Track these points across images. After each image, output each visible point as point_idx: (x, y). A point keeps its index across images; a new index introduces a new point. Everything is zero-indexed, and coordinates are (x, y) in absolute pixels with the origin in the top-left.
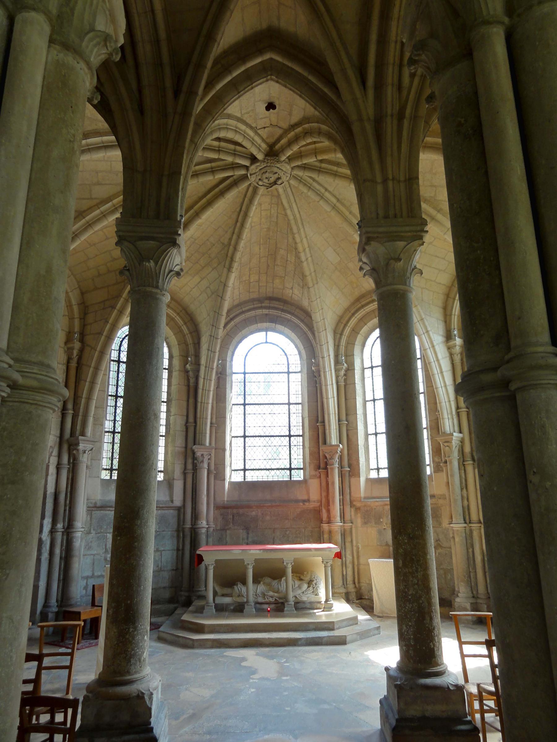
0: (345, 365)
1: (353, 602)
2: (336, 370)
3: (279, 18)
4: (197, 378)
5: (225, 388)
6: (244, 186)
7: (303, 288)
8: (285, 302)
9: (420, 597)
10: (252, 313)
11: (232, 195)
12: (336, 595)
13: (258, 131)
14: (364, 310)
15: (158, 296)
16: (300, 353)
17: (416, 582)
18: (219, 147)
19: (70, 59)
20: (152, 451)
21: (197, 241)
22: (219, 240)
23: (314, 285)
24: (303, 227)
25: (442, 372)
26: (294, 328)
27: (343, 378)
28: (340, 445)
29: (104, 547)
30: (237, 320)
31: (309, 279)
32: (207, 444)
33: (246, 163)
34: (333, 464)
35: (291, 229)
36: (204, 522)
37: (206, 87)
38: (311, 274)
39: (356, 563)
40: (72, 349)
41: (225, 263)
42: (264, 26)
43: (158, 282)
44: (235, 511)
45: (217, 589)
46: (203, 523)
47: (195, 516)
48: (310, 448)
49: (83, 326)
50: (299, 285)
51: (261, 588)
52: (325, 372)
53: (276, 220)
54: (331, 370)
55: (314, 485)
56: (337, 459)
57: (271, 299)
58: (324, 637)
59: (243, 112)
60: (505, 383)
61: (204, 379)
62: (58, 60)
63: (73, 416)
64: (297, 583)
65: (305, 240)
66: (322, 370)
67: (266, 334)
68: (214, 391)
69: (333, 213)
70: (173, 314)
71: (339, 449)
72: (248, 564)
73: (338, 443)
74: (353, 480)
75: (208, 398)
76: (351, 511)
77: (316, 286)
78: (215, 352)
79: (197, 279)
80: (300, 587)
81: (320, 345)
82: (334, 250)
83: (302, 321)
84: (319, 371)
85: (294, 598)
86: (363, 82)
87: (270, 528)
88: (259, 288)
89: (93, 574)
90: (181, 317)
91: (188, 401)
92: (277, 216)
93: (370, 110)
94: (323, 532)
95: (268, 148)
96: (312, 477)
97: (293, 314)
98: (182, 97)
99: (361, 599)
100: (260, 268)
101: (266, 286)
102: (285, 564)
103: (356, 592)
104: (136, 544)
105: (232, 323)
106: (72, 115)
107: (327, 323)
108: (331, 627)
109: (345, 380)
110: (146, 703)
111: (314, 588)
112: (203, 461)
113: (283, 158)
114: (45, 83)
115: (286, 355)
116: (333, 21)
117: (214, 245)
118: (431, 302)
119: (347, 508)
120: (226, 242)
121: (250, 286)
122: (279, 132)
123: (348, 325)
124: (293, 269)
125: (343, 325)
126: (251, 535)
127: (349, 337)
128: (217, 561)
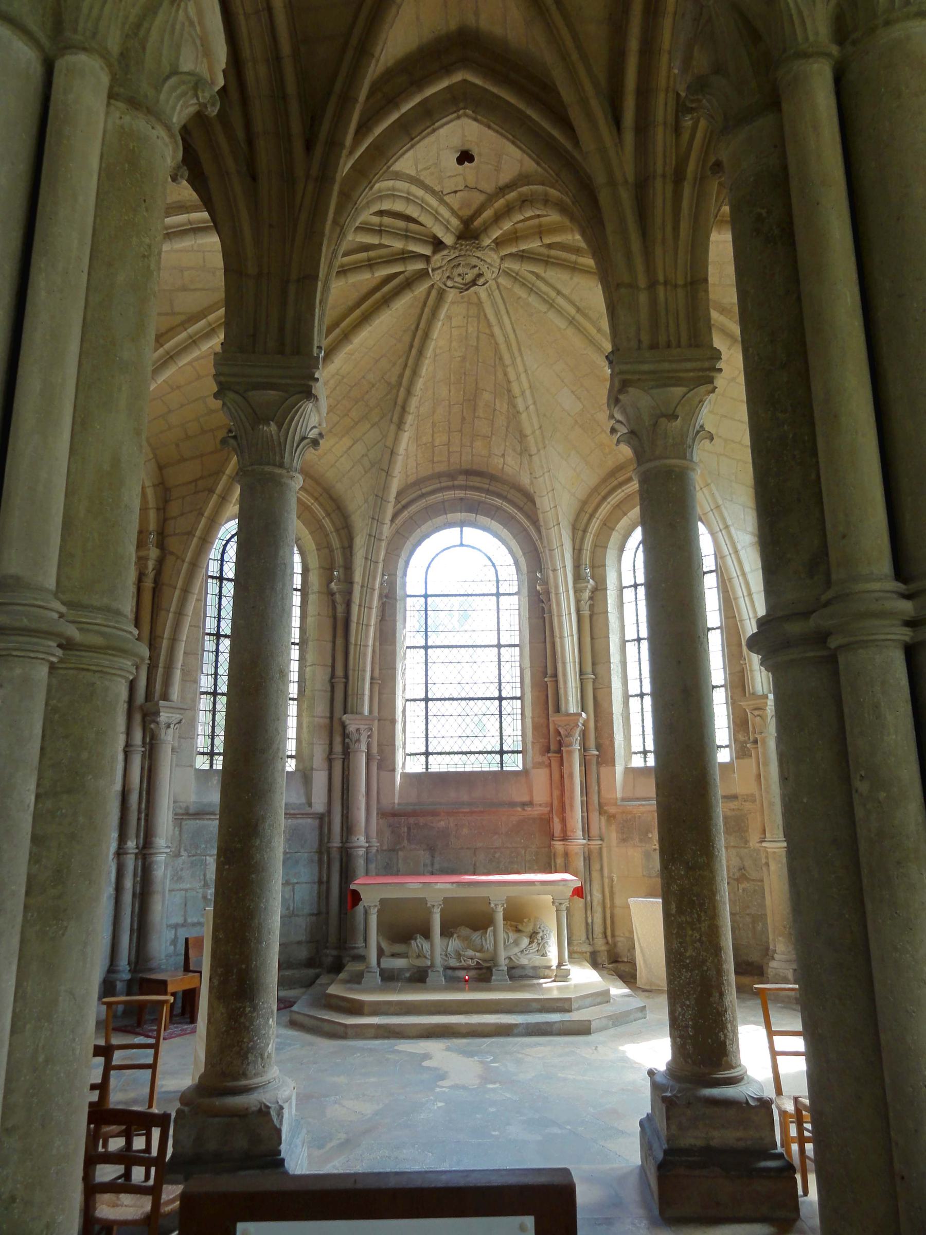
0: (591, 581)
1: (603, 967)
2: (577, 591)
3: (477, 13)
4: (348, 604)
5: (395, 621)
6: (421, 289)
7: (521, 454)
8: (492, 478)
9: (704, 962)
10: (439, 496)
11: (403, 304)
12: (575, 956)
13: (446, 198)
14: (623, 491)
15: (283, 480)
16: (516, 563)
17: (698, 937)
18: (380, 225)
19: (140, 123)
20: (277, 730)
21: (345, 380)
22: (382, 378)
23: (539, 451)
24: (521, 355)
25: (750, 594)
26: (507, 521)
28: (583, 713)
29: (202, 877)
30: (413, 508)
31: (531, 439)
32: (366, 712)
33: (426, 250)
34: (570, 745)
35: (501, 359)
36: (362, 838)
37: (357, 132)
38: (533, 432)
39: (608, 905)
40: (146, 559)
41: (392, 416)
42: (453, 25)
43: (282, 457)
44: (412, 820)
45: (384, 945)
46: (360, 840)
47: (347, 828)
48: (533, 718)
49: (163, 522)
50: (514, 450)
51: (454, 944)
52: (557, 594)
53: (475, 344)
54: (567, 591)
55: (540, 778)
56: (577, 736)
57: (468, 473)
58: (556, 1022)
59: (420, 167)
60: (821, 638)
61: (360, 605)
62: (122, 127)
63: (148, 668)
64: (512, 936)
65: (523, 377)
66: (553, 590)
67: (462, 531)
68: (375, 625)
69: (570, 332)
71: (581, 721)
72: (433, 906)
74: (604, 770)
75: (367, 637)
76: (600, 820)
77: (542, 452)
78: (377, 562)
79: (346, 442)
80: (516, 943)
81: (550, 550)
82: (573, 392)
83: (520, 509)
84: (548, 593)
85: (507, 961)
86: (617, 121)
87: (468, 848)
88: (449, 456)
89: (185, 920)
90: (321, 505)
91: (334, 642)
92: (478, 338)
93: (627, 168)
94: (555, 855)
95: (462, 226)
96: (537, 765)
97: (505, 498)
99: (616, 961)
100: (450, 423)
101: (461, 451)
102: (492, 905)
103: (608, 951)
104: (253, 876)
105: (405, 514)
106: (145, 214)
107: (560, 513)
108: (566, 1006)
109: (592, 607)
110: (273, 1121)
111: (539, 944)
112: (358, 741)
113: (487, 242)
114: (104, 165)
115: (494, 565)
117: (373, 386)
118: (733, 478)
119: (594, 816)
120: (394, 380)
121: (433, 452)
122: (481, 198)
123: (597, 516)
124: (505, 424)
125: (587, 516)
126: (437, 859)
127: (598, 535)
128: (382, 901)
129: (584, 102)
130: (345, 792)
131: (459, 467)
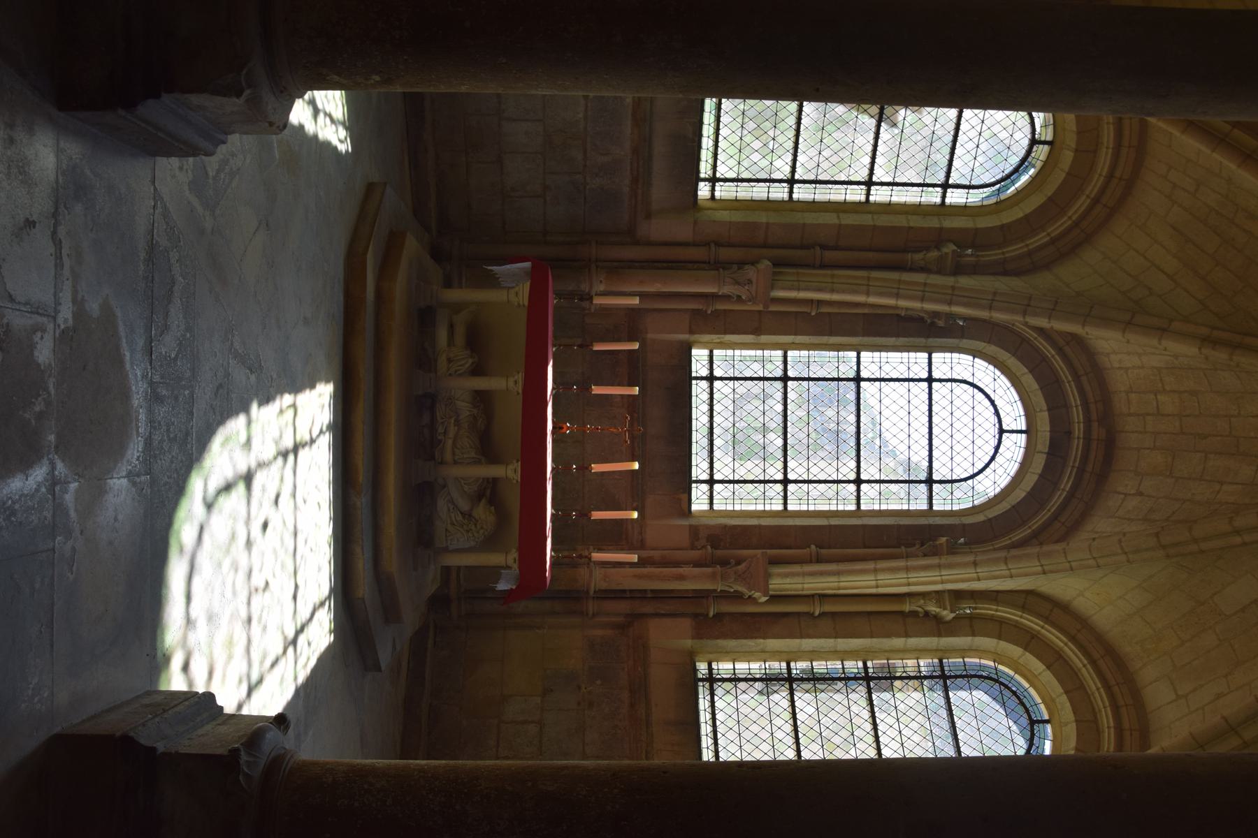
0: (953, 615)
8: (1102, 477)
10: (1074, 398)
14: (1084, 666)
23: (1164, 547)
27: (919, 609)
30: (1058, 363)
54: (942, 582)
57: (1110, 444)
67: (1021, 432)
70: (1076, 212)
71: (757, 595)
73: (771, 593)
74: (686, 624)
78: (991, 308)
81: (1006, 558)
83: (1055, 517)
84: (935, 552)
88: (1138, 415)
105: (1049, 351)
109: (914, 614)
115: (972, 477)
119: (623, 607)
127: (1017, 626)
130: (665, 265)
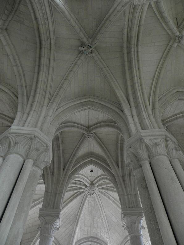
6: (83, 195)
8: (98, 239)
11: (78, 198)
13: (88, 178)
19: (37, 169)
35: (99, 209)
37: (72, 168)
50: (103, 231)
57: (92, 237)
65: (104, 214)
69: (113, 204)
77: (109, 232)
93: (120, 173)
98: (65, 170)
113: (96, 186)
116: (108, 151)
120: (76, 214)
122: (95, 178)
129: (112, 163)
131: (90, 236)
